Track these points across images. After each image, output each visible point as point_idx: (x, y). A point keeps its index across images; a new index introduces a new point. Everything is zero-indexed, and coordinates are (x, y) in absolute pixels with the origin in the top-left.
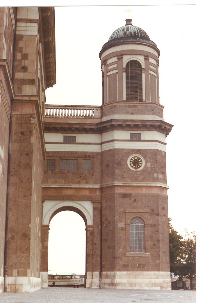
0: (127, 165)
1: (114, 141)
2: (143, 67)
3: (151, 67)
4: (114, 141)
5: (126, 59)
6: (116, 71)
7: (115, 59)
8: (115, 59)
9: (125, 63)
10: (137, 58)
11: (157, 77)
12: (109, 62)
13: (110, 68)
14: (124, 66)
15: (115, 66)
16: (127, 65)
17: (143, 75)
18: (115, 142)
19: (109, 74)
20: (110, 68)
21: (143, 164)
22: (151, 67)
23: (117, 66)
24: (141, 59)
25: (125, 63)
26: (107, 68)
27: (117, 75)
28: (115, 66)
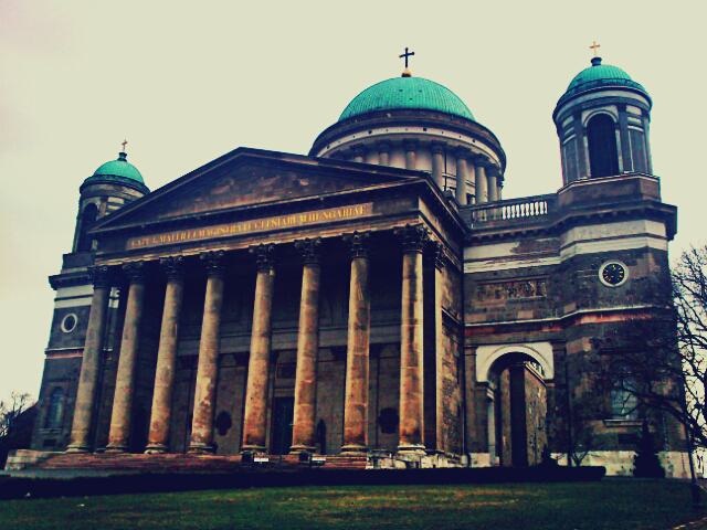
1: (575, 243)
3: (630, 119)
7: (571, 119)
11: (644, 134)
17: (617, 132)
18: (577, 245)
22: (630, 119)
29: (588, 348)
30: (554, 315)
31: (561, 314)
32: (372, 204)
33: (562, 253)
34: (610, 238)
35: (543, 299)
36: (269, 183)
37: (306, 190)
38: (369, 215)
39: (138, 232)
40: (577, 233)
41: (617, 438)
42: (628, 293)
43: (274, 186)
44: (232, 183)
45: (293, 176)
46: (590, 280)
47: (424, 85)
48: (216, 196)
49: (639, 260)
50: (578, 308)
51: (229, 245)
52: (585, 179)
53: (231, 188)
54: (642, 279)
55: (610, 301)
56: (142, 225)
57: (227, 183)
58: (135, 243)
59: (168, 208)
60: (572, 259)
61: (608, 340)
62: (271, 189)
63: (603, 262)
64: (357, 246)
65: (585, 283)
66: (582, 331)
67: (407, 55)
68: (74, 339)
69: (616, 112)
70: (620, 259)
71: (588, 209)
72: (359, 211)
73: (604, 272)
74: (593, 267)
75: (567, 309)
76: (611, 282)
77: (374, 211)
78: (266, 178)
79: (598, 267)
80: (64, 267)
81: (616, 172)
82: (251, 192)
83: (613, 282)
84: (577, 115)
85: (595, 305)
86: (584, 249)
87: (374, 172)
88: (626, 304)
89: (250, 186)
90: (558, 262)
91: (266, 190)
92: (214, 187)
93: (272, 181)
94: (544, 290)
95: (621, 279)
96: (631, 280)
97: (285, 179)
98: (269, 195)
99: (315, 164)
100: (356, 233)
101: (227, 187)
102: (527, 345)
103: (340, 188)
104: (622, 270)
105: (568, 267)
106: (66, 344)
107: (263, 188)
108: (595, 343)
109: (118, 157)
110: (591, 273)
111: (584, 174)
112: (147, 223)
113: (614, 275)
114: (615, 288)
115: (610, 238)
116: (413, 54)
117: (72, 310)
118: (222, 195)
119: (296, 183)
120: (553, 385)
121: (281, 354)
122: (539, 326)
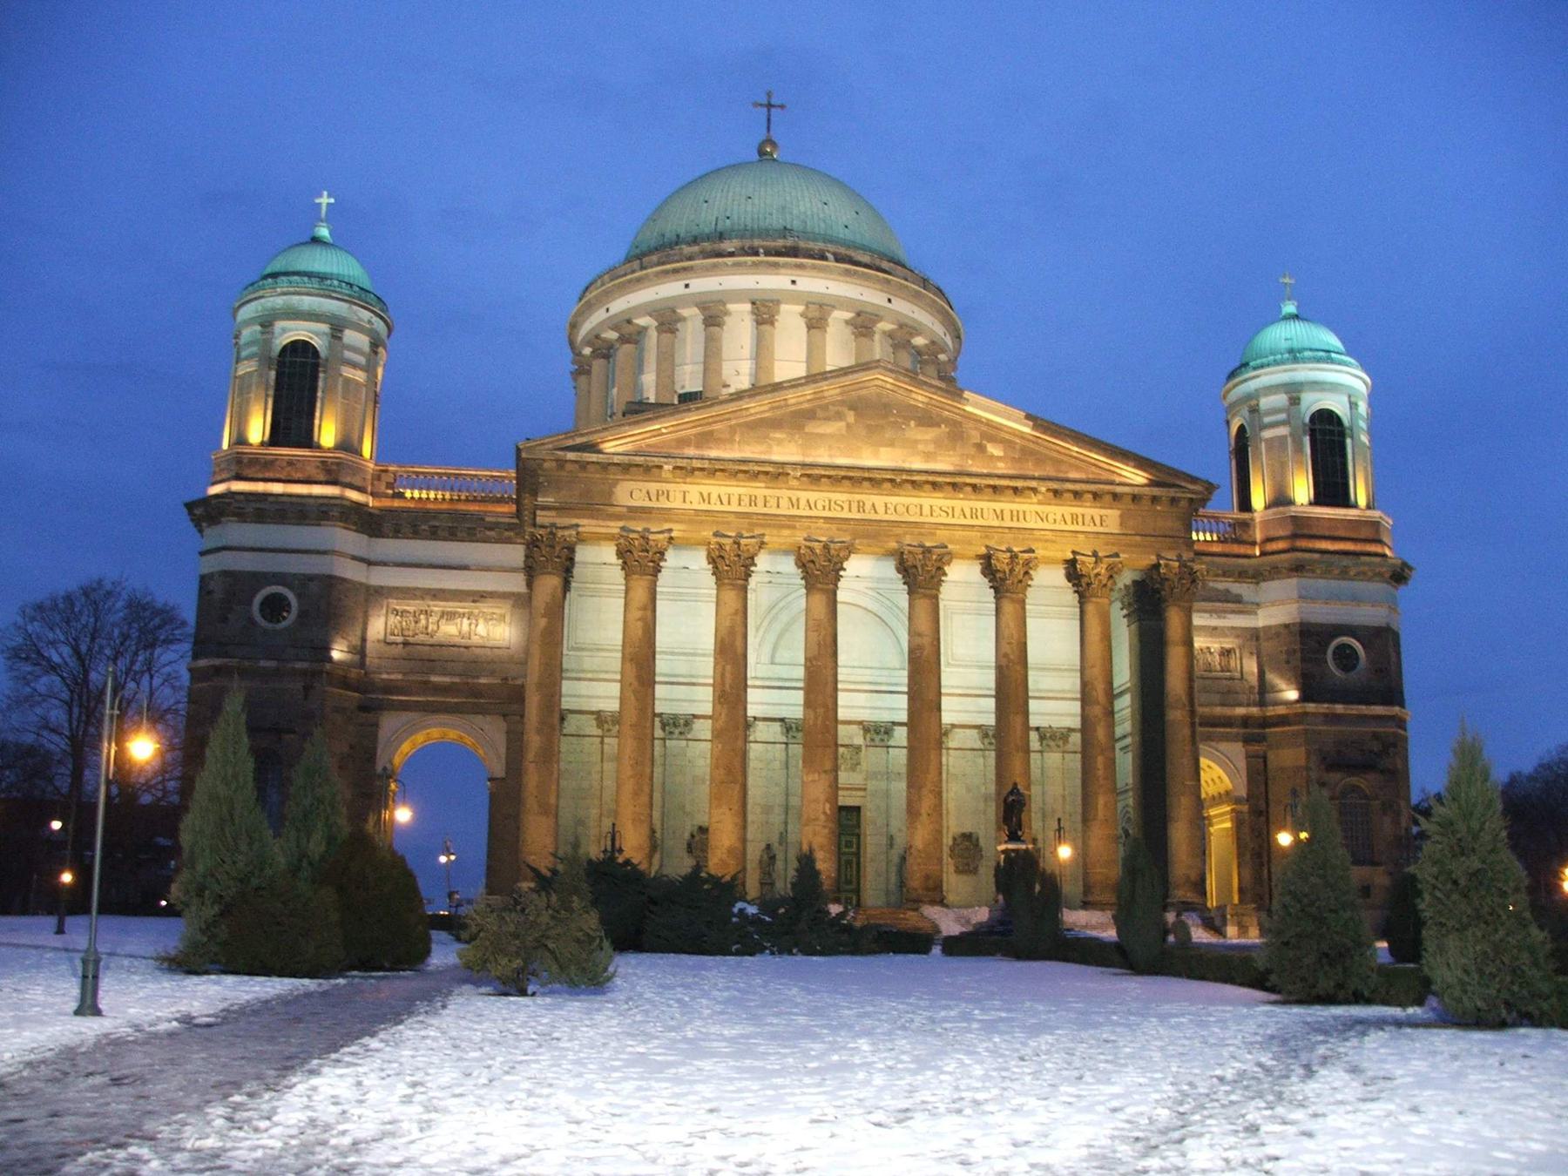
2: (1346, 422)
8: (1281, 399)
14: (1307, 420)
17: (1348, 441)
20: (1267, 420)
23: (1289, 416)
28: (1283, 416)
44: (851, 417)
48: (822, 436)
53: (848, 426)
57: (839, 416)
67: (770, 106)
79: (1327, 645)
89: (889, 434)
98: (928, 456)
101: (842, 424)
102: (1213, 744)
107: (916, 442)
116: (782, 107)
119: (981, 448)
122: (1228, 722)
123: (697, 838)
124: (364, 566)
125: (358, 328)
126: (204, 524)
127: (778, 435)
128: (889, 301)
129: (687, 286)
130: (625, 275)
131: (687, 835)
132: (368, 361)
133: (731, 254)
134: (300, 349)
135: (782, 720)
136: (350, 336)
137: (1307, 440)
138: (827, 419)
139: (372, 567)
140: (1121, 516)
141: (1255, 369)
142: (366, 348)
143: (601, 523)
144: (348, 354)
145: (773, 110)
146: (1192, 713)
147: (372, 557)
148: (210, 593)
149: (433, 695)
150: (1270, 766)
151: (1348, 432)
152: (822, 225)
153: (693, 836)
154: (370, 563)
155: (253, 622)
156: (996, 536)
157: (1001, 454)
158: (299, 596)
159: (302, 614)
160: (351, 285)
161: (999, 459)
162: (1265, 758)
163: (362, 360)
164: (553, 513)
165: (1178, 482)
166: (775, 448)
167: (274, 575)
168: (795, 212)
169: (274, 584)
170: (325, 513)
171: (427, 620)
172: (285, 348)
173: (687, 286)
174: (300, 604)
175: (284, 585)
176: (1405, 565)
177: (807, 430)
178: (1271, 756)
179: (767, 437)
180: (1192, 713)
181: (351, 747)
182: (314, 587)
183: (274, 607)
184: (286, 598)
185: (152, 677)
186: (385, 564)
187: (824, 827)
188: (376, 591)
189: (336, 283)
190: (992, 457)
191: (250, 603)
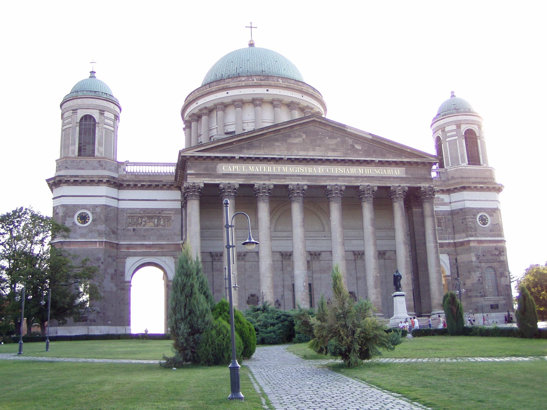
0: (477, 222)
1: (464, 200)
4: (464, 200)
5: (464, 128)
6: (456, 137)
8: (454, 127)
9: (463, 131)
10: (474, 128)
12: (447, 129)
13: (448, 134)
15: (455, 133)
16: (465, 133)
17: (479, 141)
19: (447, 140)
20: (448, 134)
21: (489, 221)
23: (456, 133)
24: (475, 128)
25: (463, 131)
26: (446, 134)
27: (457, 141)
28: (455, 133)
29: (474, 259)
30: (449, 239)
31: (454, 239)
32: (404, 169)
33: (452, 204)
34: (481, 200)
35: (442, 230)
36: (333, 143)
37: (361, 152)
38: (404, 176)
39: (231, 160)
40: (466, 195)
41: (490, 306)
42: (491, 231)
43: (337, 144)
44: (304, 136)
45: (350, 141)
46: (473, 222)
47: (266, 52)
48: (293, 144)
49: (494, 214)
50: (467, 237)
51: (308, 181)
52: (464, 164)
54: (496, 224)
55: (484, 236)
56: (237, 156)
57: (300, 136)
58: (224, 168)
59: (250, 147)
60: (461, 209)
61: (484, 255)
62: (334, 147)
63: (478, 213)
64: (400, 194)
65: (470, 223)
66: (469, 250)
67: (251, 27)
68: (91, 231)
69: (477, 129)
70: (488, 213)
71: (473, 183)
72: (398, 172)
73: (479, 219)
74: (474, 216)
75: (457, 236)
76: (483, 224)
77: (406, 173)
78: (330, 137)
79: (476, 215)
80: (58, 168)
81: (480, 165)
82: (320, 146)
83: (484, 224)
84: (459, 126)
85: (476, 236)
86: (469, 205)
87: (409, 150)
88: (491, 236)
89: (318, 142)
90: (450, 209)
91: (331, 147)
92: (290, 136)
93: (334, 142)
94: (442, 225)
95: (487, 223)
96: (491, 224)
97: (344, 142)
98: (334, 150)
99: (370, 137)
100: (399, 186)
101: (301, 139)
103: (383, 156)
104: (487, 218)
105: (458, 213)
106: (83, 235)
107: (329, 145)
108: (478, 257)
109: (89, 75)
110: (473, 218)
111: (463, 162)
112: (241, 156)
113: (484, 220)
114: (484, 227)
115: (481, 200)
117: (84, 207)
118: (297, 144)
119: (353, 146)
120: (450, 278)
121: (323, 253)
123: (250, 299)
124: (117, 201)
125: (110, 111)
126: (53, 187)
127: (277, 144)
128: (302, 96)
129: (227, 93)
130: (204, 90)
131: (247, 298)
132: (114, 123)
133: (244, 81)
134: (87, 118)
135: (280, 252)
136: (106, 114)
137: (464, 140)
138: (296, 137)
139: (120, 202)
140: (405, 170)
141: (443, 116)
142: (113, 117)
143: (212, 179)
144: (106, 121)
145: (252, 28)
146: (436, 242)
147: (120, 198)
148: (57, 214)
149: (146, 249)
150: (459, 261)
151: (478, 138)
152: (276, 70)
153: (249, 298)
154: (118, 200)
155: (74, 223)
156: (361, 179)
157: (360, 148)
158: (93, 213)
159: (93, 220)
160: (107, 94)
161: (360, 150)
162: (456, 259)
163: (112, 123)
164: (194, 176)
165: (426, 157)
166: (277, 149)
167: (82, 205)
168: (266, 65)
169: (82, 209)
170: (102, 181)
171: (141, 220)
172: (82, 119)
173: (227, 93)
174: (93, 217)
175: (86, 209)
176: (502, 186)
177: (288, 141)
178: (458, 257)
179: (274, 145)
180: (436, 242)
181: (115, 271)
182: (98, 210)
183: (83, 218)
184: (87, 214)
185: (31, 247)
186: (125, 200)
187: (304, 292)
188: (121, 210)
189: (100, 93)
190: (357, 149)
191: (73, 216)
